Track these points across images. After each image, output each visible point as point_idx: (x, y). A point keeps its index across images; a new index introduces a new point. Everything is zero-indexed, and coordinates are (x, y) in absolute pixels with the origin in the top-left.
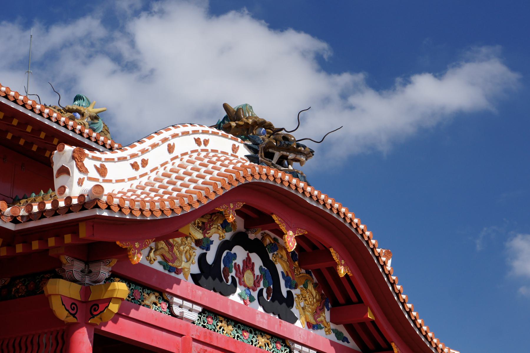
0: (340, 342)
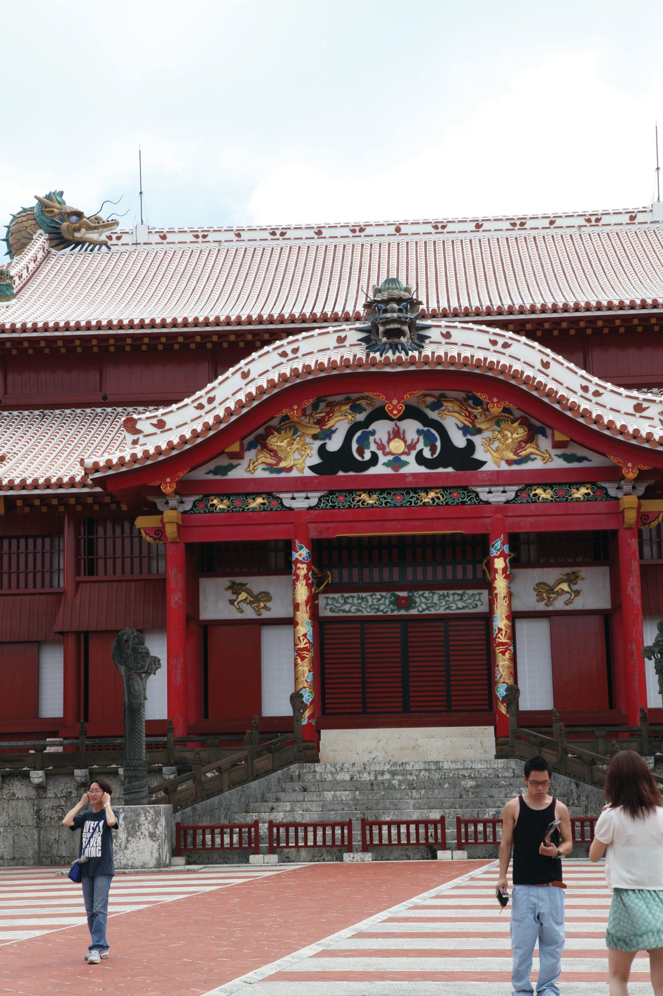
0: (575, 465)
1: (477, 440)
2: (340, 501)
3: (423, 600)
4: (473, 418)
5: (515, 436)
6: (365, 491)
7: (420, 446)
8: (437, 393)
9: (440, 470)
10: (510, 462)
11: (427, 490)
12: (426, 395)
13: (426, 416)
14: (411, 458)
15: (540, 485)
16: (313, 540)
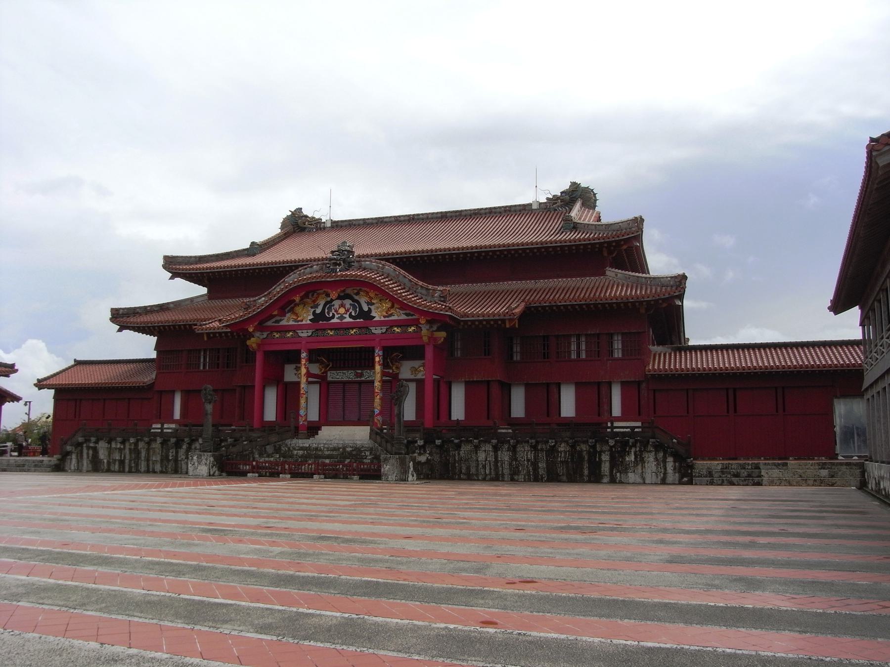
0: (410, 317)
1: (372, 307)
2: (320, 333)
3: (367, 374)
4: (371, 298)
5: (387, 305)
6: (329, 329)
7: (351, 311)
8: (358, 288)
9: (358, 320)
10: (385, 317)
11: (352, 329)
12: (354, 289)
13: (354, 298)
14: (347, 316)
15: (396, 326)
16: (308, 349)
